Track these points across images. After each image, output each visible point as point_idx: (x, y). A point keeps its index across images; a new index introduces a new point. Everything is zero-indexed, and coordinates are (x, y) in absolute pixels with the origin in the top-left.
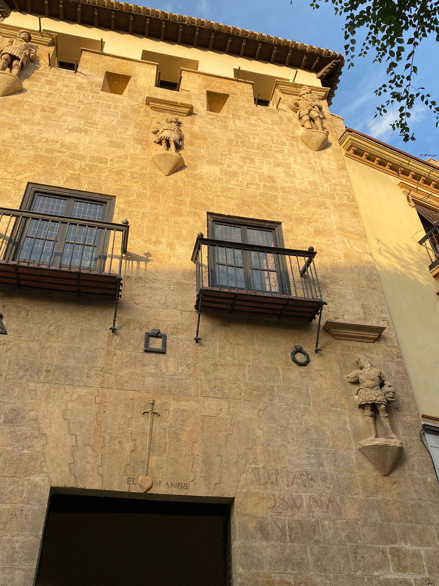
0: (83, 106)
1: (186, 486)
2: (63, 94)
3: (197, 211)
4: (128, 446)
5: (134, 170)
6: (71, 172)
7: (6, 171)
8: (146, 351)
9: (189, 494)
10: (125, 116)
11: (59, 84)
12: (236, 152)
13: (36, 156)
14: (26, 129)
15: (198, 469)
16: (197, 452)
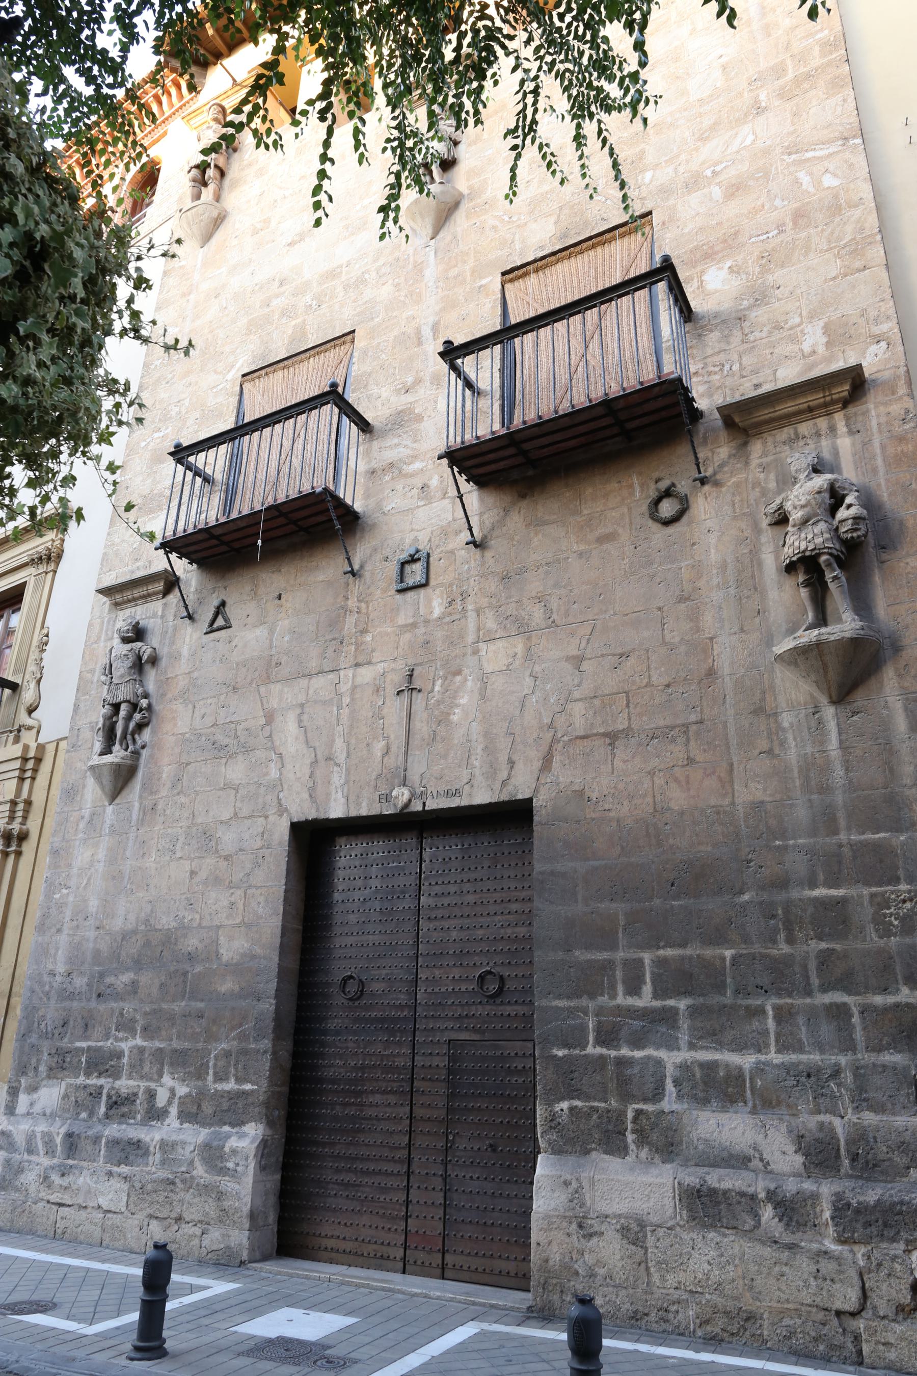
1: (457, 793)
3: (484, 282)
4: (379, 747)
6: (293, 323)
7: (216, 372)
8: (400, 591)
9: (463, 804)
15: (477, 763)
16: (475, 737)
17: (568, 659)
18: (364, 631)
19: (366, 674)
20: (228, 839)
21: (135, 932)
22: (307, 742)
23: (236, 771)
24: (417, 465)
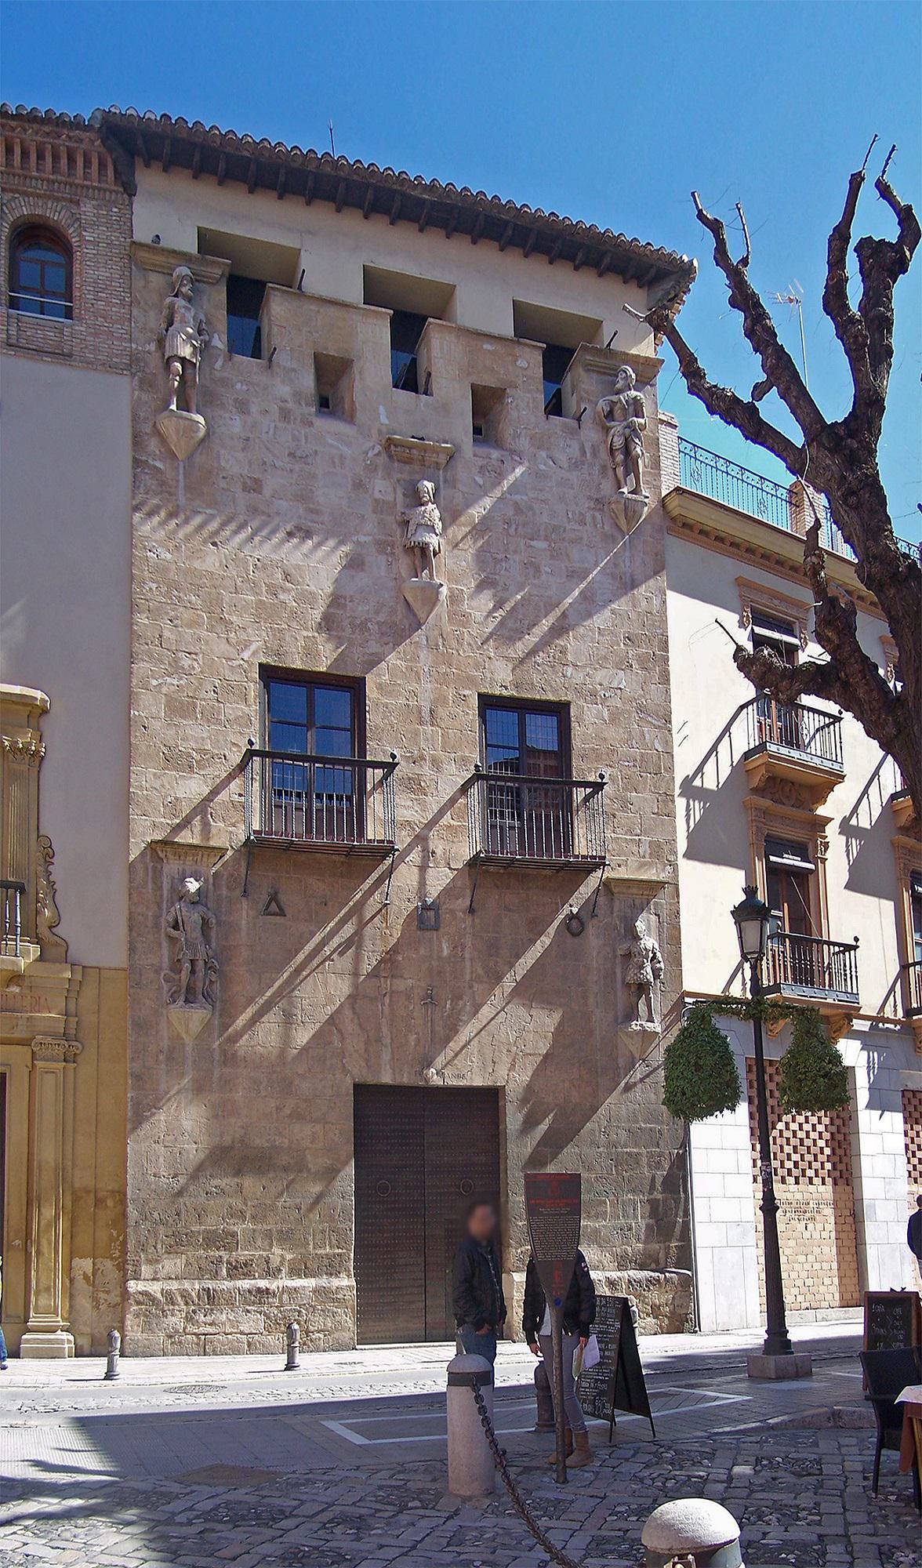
0: (297, 468)
2: (264, 436)
4: (412, 1038)
5: (381, 618)
6: (305, 633)
10: (359, 485)
11: (254, 409)
12: (515, 552)
20: (304, 1087)
21: (231, 1148)
22: (360, 1025)
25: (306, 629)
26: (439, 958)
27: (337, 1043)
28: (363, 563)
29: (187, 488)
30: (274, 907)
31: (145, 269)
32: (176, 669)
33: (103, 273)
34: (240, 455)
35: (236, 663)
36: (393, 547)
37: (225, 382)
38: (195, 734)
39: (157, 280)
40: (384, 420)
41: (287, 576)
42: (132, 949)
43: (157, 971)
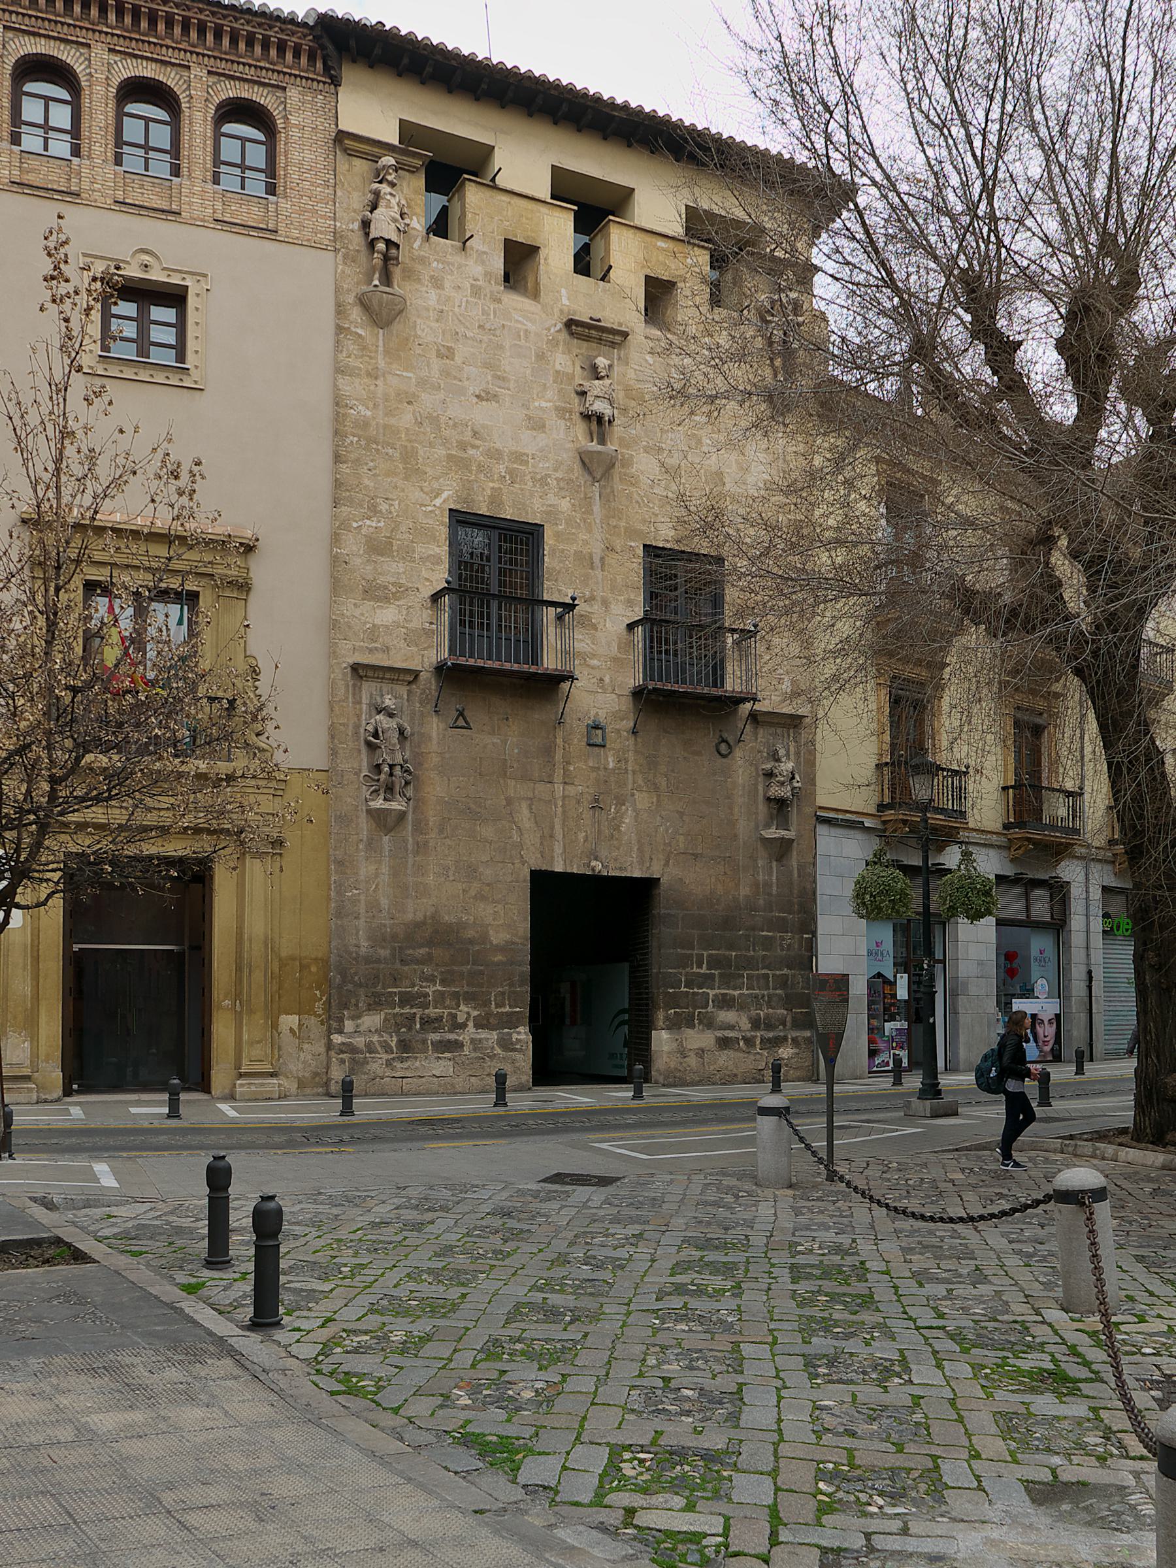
0: (485, 338)
2: (456, 309)
3: (633, 544)
5: (559, 475)
6: (491, 485)
10: (541, 357)
11: (447, 285)
13: (450, 457)
14: (428, 401)
17: (678, 812)
18: (568, 763)
19: (571, 790)
20: (488, 873)
23: (488, 831)
24: (595, 662)
25: (493, 481)
26: (605, 769)
27: (516, 838)
28: (544, 426)
29: (387, 352)
30: (461, 723)
31: (349, 153)
32: (374, 510)
33: (309, 156)
34: (435, 325)
35: (430, 508)
36: (571, 412)
37: (422, 260)
38: (392, 570)
39: (360, 166)
40: (565, 301)
41: (475, 434)
42: (334, 752)
43: (357, 774)
